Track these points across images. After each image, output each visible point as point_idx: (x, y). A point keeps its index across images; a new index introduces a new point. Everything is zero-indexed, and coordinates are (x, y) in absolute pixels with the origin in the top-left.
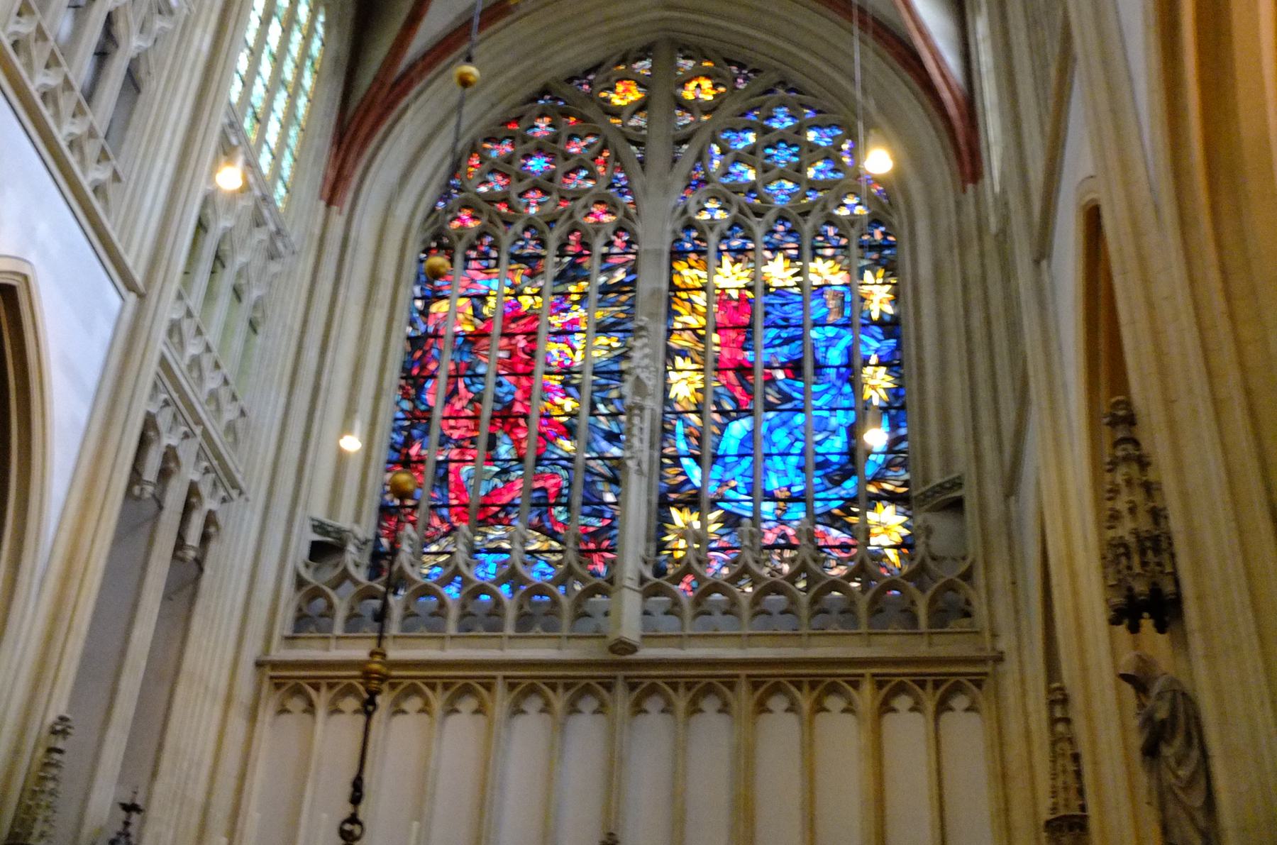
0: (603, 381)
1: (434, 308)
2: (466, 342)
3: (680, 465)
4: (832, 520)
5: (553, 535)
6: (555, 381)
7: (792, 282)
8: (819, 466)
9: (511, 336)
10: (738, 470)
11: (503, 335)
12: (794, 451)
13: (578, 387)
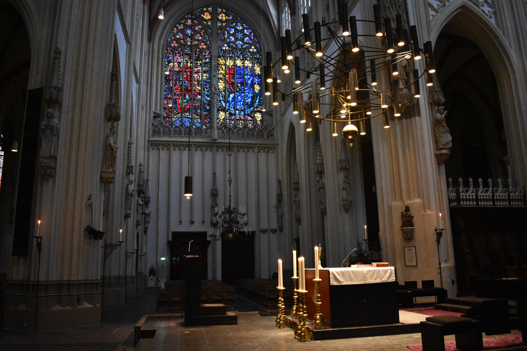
0: (206, 84)
1: (170, 65)
2: (177, 73)
3: (221, 102)
4: (249, 115)
5: (198, 115)
6: (196, 83)
7: (241, 65)
8: (247, 104)
9: (187, 72)
10: (232, 104)
11: (185, 72)
12: (242, 101)
13: (200, 84)
